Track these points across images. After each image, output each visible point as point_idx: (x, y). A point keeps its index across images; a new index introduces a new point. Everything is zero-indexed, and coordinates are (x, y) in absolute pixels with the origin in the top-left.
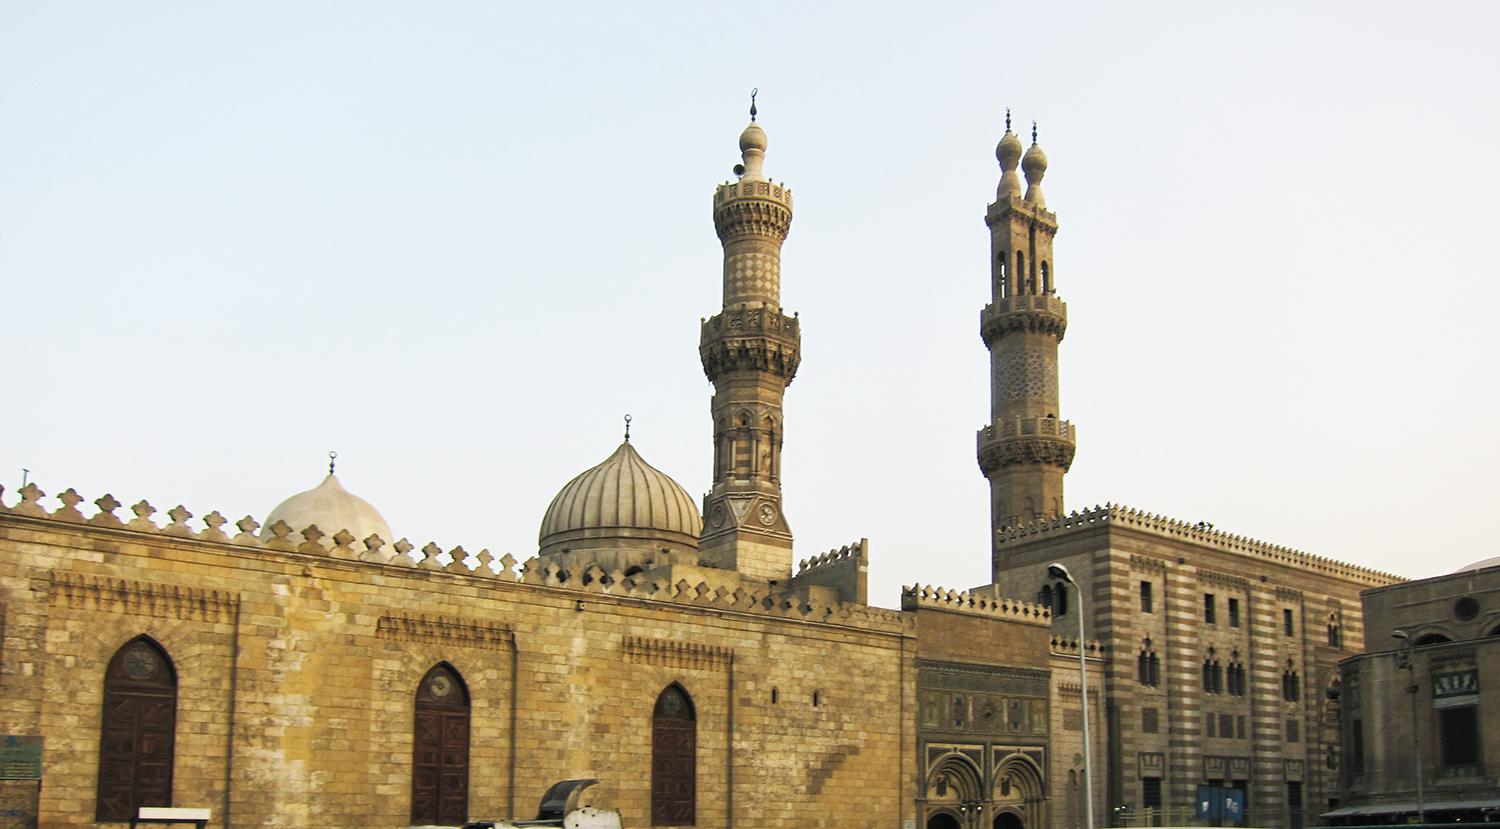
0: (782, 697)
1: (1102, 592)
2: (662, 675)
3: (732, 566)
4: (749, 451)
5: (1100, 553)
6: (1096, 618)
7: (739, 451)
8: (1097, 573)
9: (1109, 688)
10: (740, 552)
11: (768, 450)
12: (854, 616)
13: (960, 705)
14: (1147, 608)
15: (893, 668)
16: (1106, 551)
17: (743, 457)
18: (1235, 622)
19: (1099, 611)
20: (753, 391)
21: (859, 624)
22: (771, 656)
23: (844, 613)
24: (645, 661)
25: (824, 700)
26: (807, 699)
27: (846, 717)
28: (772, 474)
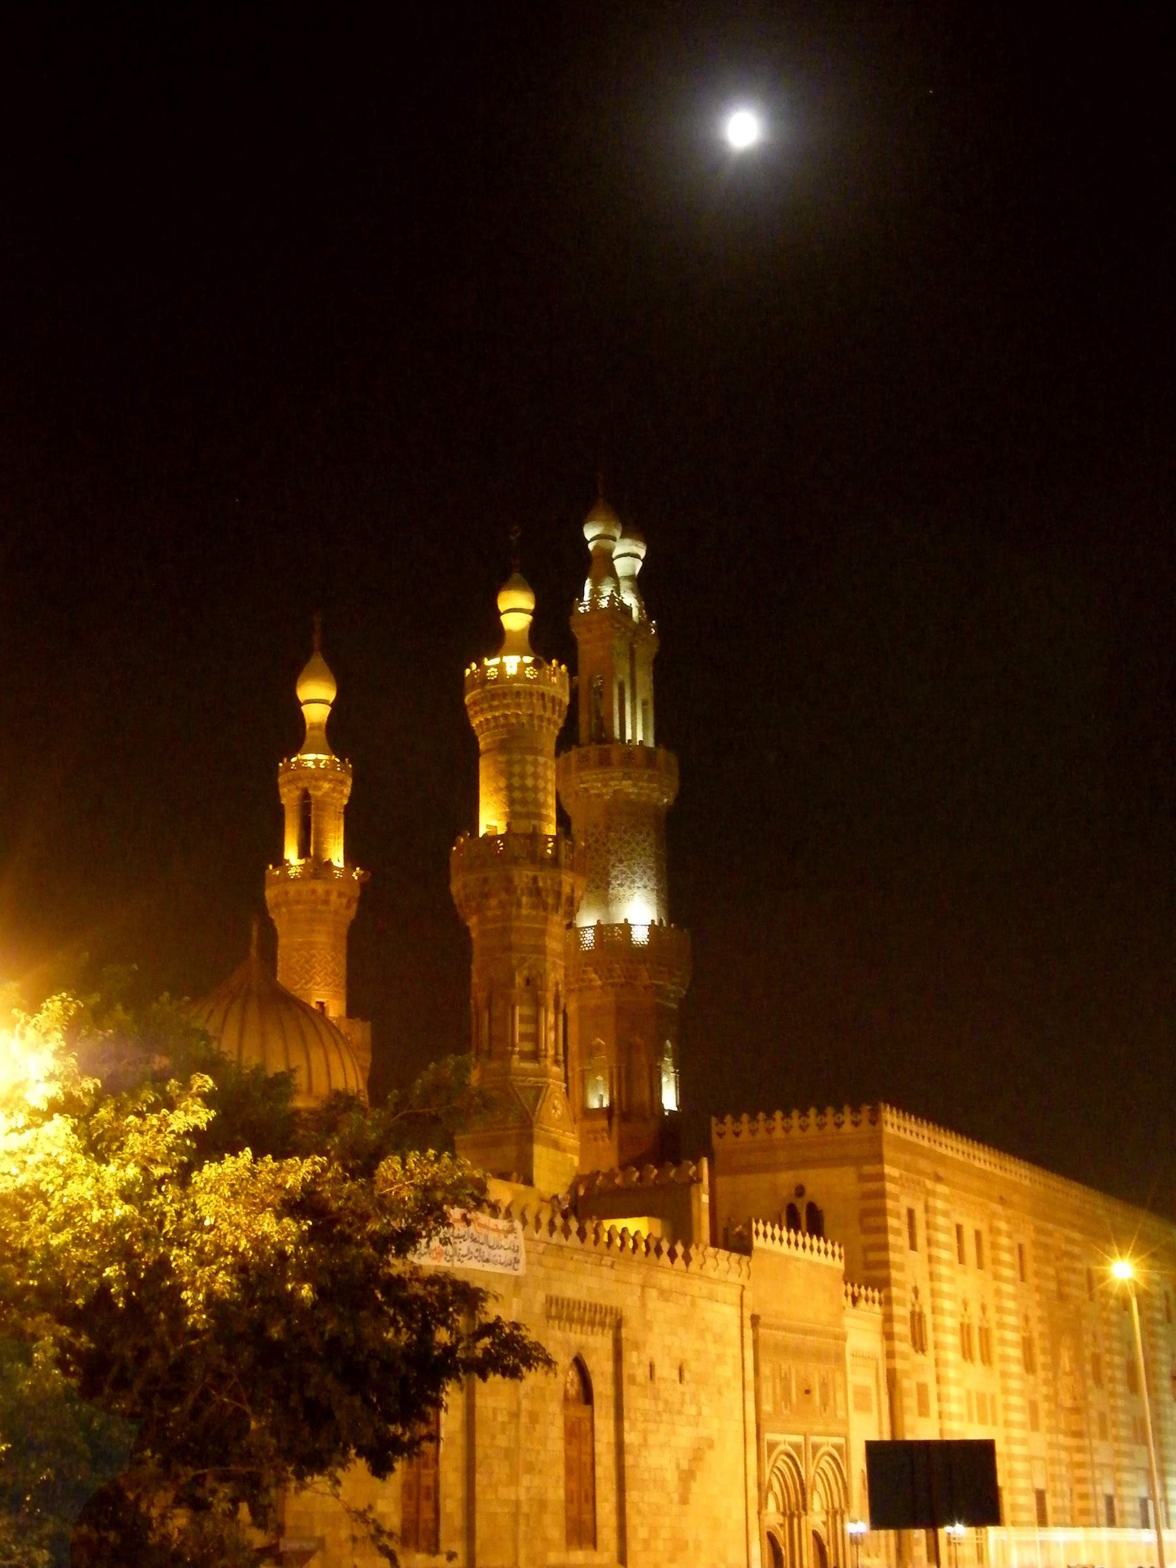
0: (658, 1372)
1: (872, 1221)
2: (568, 1342)
3: (529, 1181)
6: (865, 1256)
8: (867, 1196)
9: (890, 1355)
10: (536, 1161)
13: (785, 1380)
14: (913, 1247)
15: (735, 1332)
16: (879, 1167)
17: (530, 1029)
18: (980, 1266)
19: (867, 1249)
22: (648, 1317)
24: (556, 1327)
25: (687, 1375)
26: (676, 1376)
27: (703, 1398)
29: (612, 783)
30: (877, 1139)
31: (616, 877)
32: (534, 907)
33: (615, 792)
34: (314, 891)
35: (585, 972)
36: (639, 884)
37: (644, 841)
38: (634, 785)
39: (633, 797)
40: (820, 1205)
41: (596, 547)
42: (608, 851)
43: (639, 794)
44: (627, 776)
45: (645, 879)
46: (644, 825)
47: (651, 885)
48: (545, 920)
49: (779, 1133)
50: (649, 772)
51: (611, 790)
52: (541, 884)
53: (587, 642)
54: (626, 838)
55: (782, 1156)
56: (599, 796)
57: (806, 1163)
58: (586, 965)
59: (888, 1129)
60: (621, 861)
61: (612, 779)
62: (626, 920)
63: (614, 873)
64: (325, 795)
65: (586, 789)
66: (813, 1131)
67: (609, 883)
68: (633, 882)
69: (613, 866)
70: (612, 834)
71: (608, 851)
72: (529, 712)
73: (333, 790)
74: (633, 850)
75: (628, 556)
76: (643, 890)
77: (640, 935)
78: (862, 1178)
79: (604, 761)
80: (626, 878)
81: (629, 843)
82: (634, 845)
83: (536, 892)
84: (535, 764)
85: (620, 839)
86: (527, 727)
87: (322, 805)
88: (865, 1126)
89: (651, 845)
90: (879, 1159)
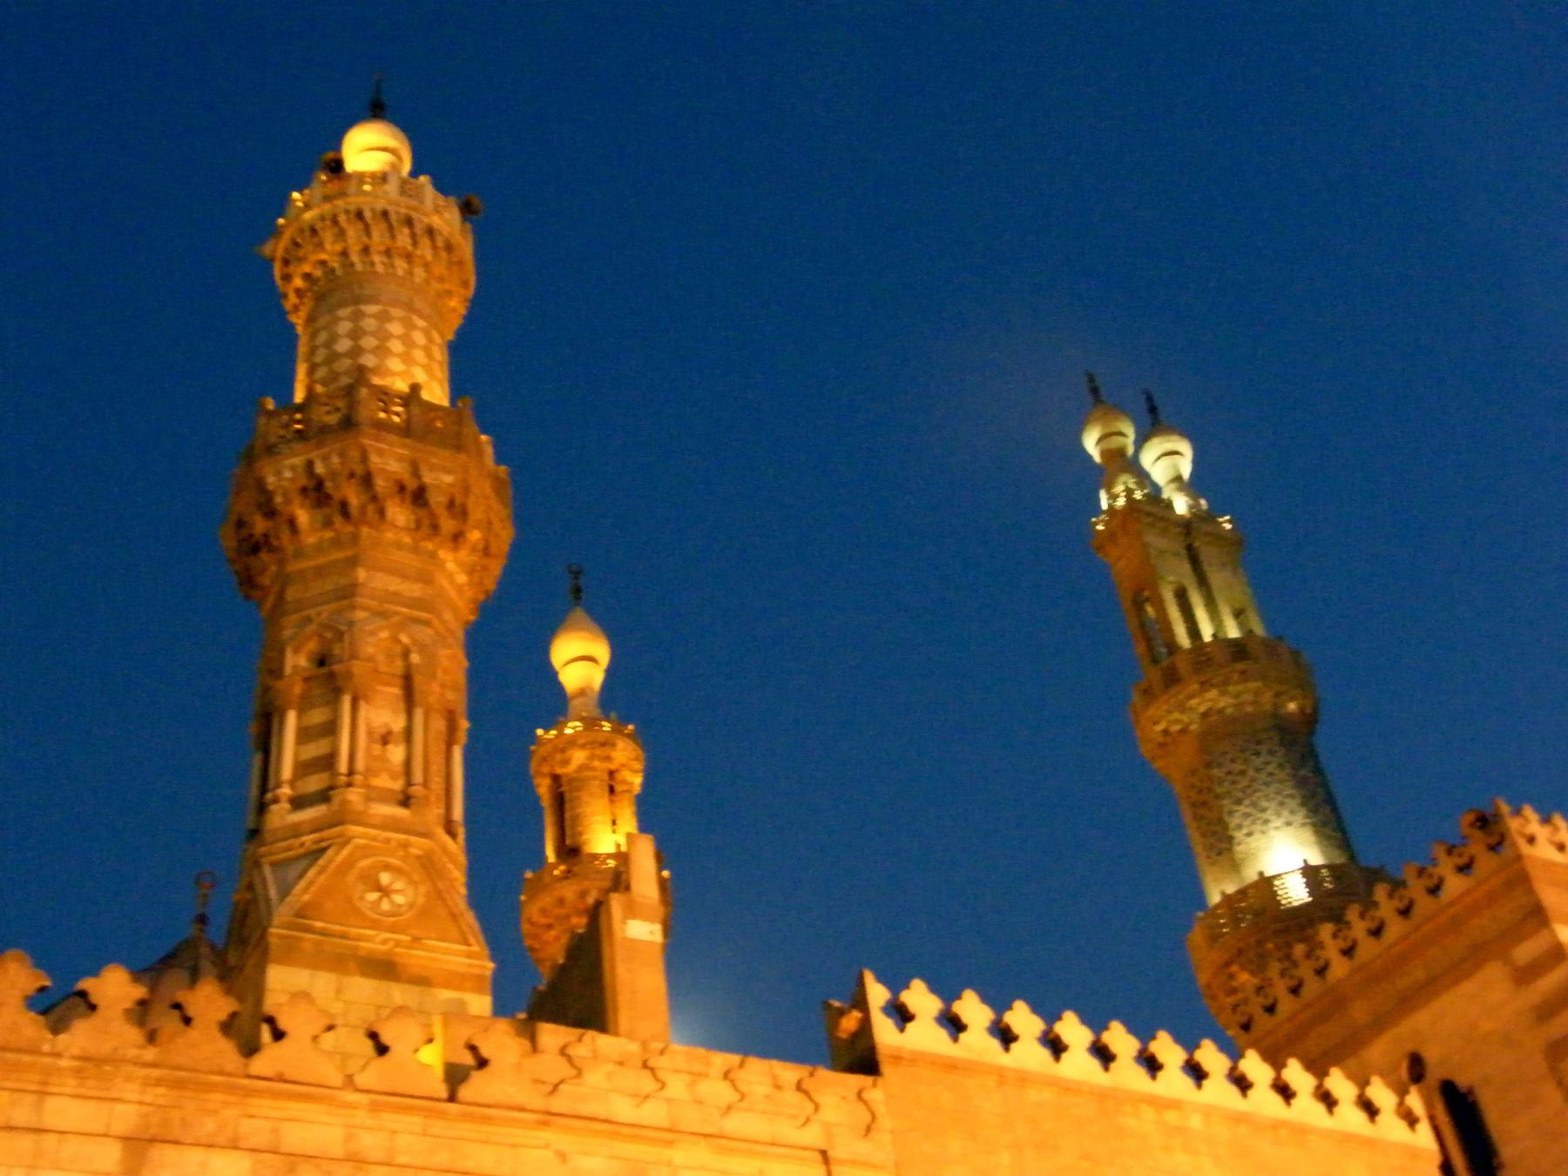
4: (331, 729)
5: (1525, 952)
7: (304, 735)
11: (398, 724)
12: (595, 1078)
16: (1545, 933)
20: (343, 581)
21: (623, 1109)
23: (549, 1064)
28: (409, 784)
29: (1193, 702)
30: (1519, 878)
31: (1240, 827)
32: (328, 524)
33: (1205, 715)
34: (561, 901)
35: (1232, 976)
36: (1278, 822)
37: (1268, 763)
38: (1223, 693)
39: (1229, 711)
40: (1462, 1081)
41: (1103, 454)
42: (1218, 797)
43: (1238, 706)
44: (1205, 685)
45: (1285, 813)
46: (1259, 743)
47: (1299, 817)
48: (355, 539)
49: (1339, 968)
50: (1240, 666)
51: (1195, 717)
52: (320, 469)
53: (1119, 560)
54: (1238, 767)
55: (1359, 1012)
56: (1183, 731)
57: (1408, 1002)
58: (1227, 964)
59: (1544, 851)
60: (1239, 802)
61: (1191, 697)
62: (1261, 874)
63: (1234, 821)
64: (583, 768)
65: (1166, 732)
66: (1396, 929)
67: (1230, 839)
68: (1266, 822)
69: (1231, 813)
70: (1216, 772)
71: (1218, 797)
72: (338, 248)
73: (592, 757)
74: (1253, 780)
75: (1168, 462)
76: (1289, 829)
77: (1295, 892)
78: (1525, 975)
79: (1172, 678)
80: (1253, 823)
81: (1243, 773)
82: (1251, 773)
83: (317, 492)
84: (358, 316)
85: (1229, 773)
86: (339, 272)
87: (578, 782)
88: (1486, 863)
89: (1281, 766)
90: (1538, 916)
